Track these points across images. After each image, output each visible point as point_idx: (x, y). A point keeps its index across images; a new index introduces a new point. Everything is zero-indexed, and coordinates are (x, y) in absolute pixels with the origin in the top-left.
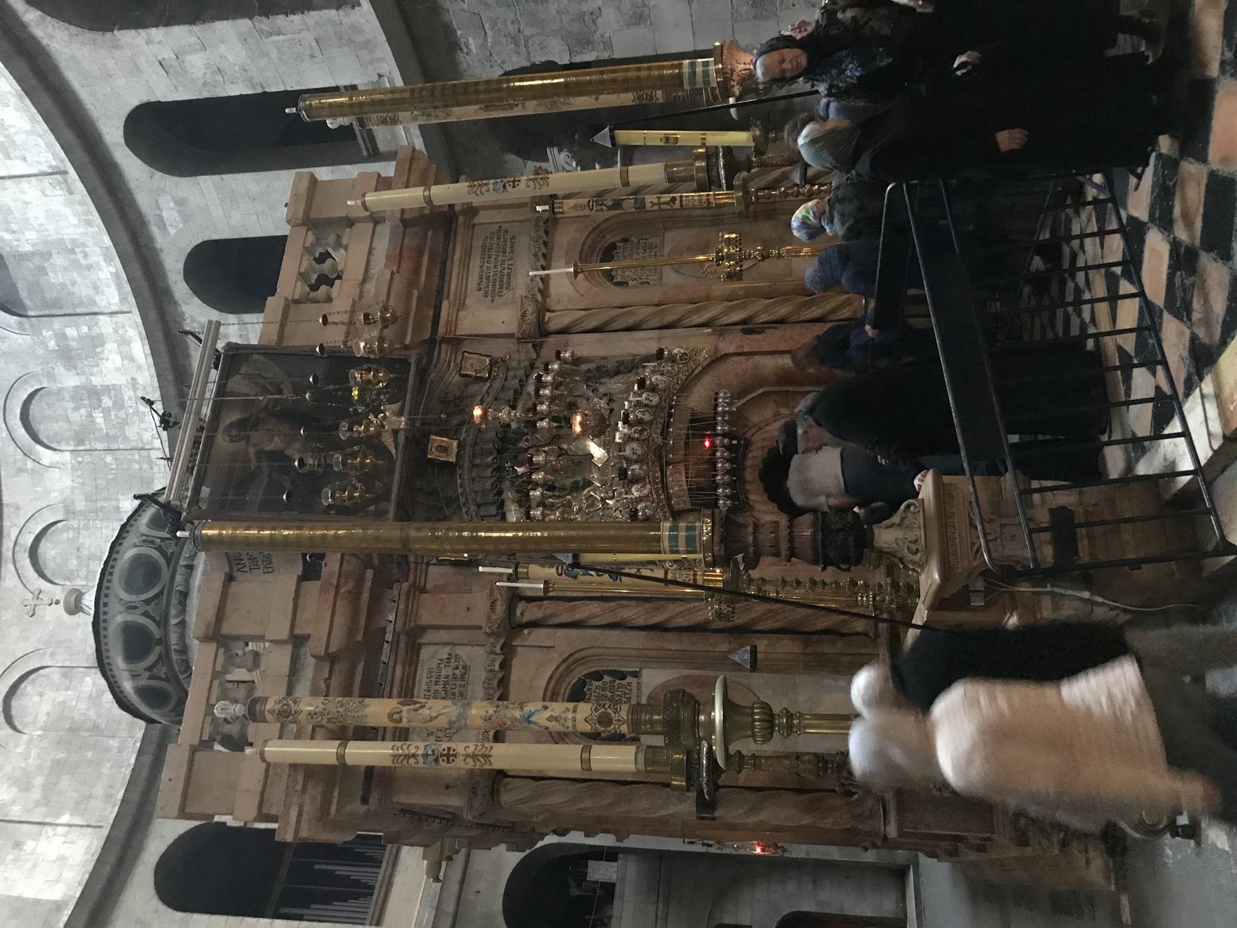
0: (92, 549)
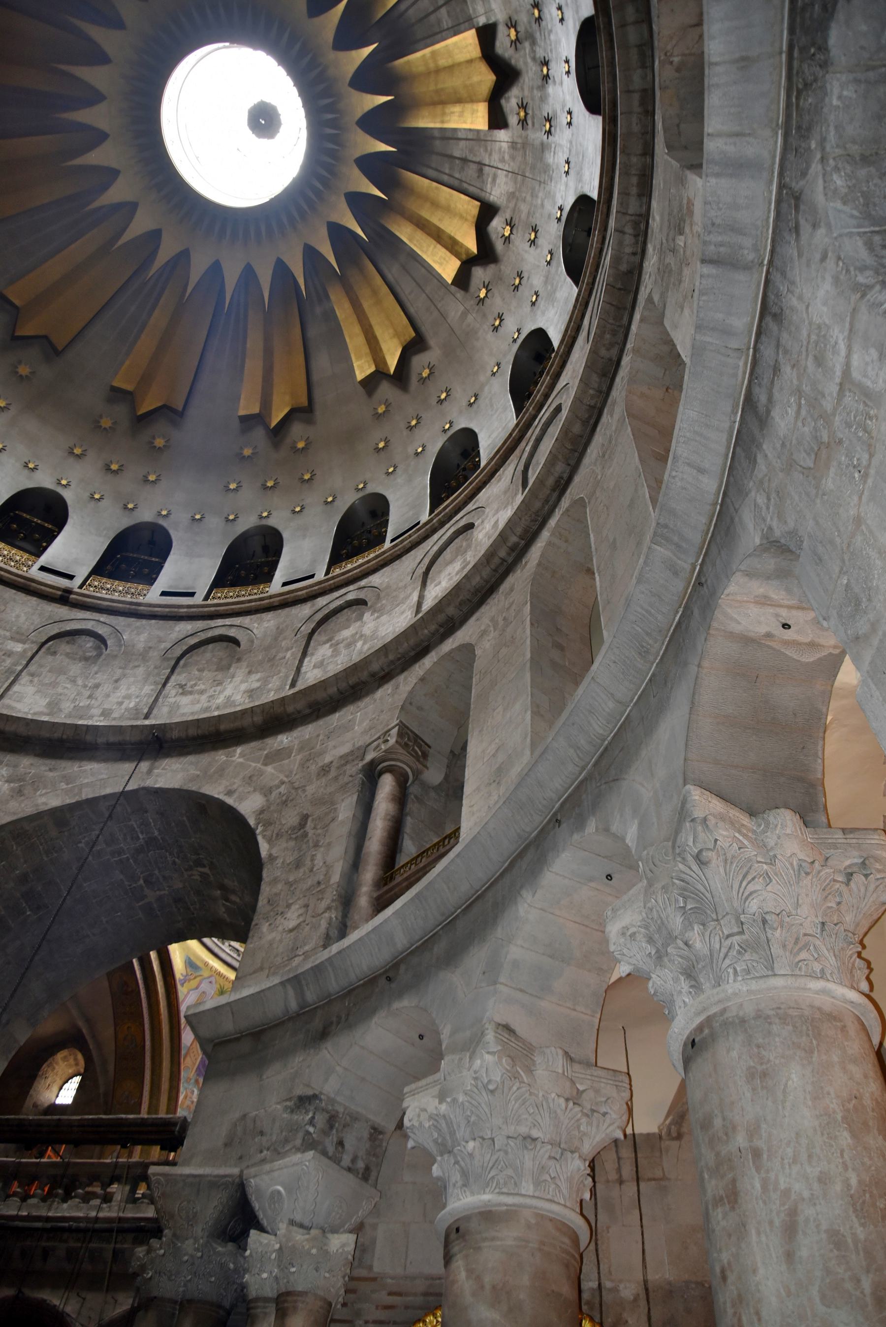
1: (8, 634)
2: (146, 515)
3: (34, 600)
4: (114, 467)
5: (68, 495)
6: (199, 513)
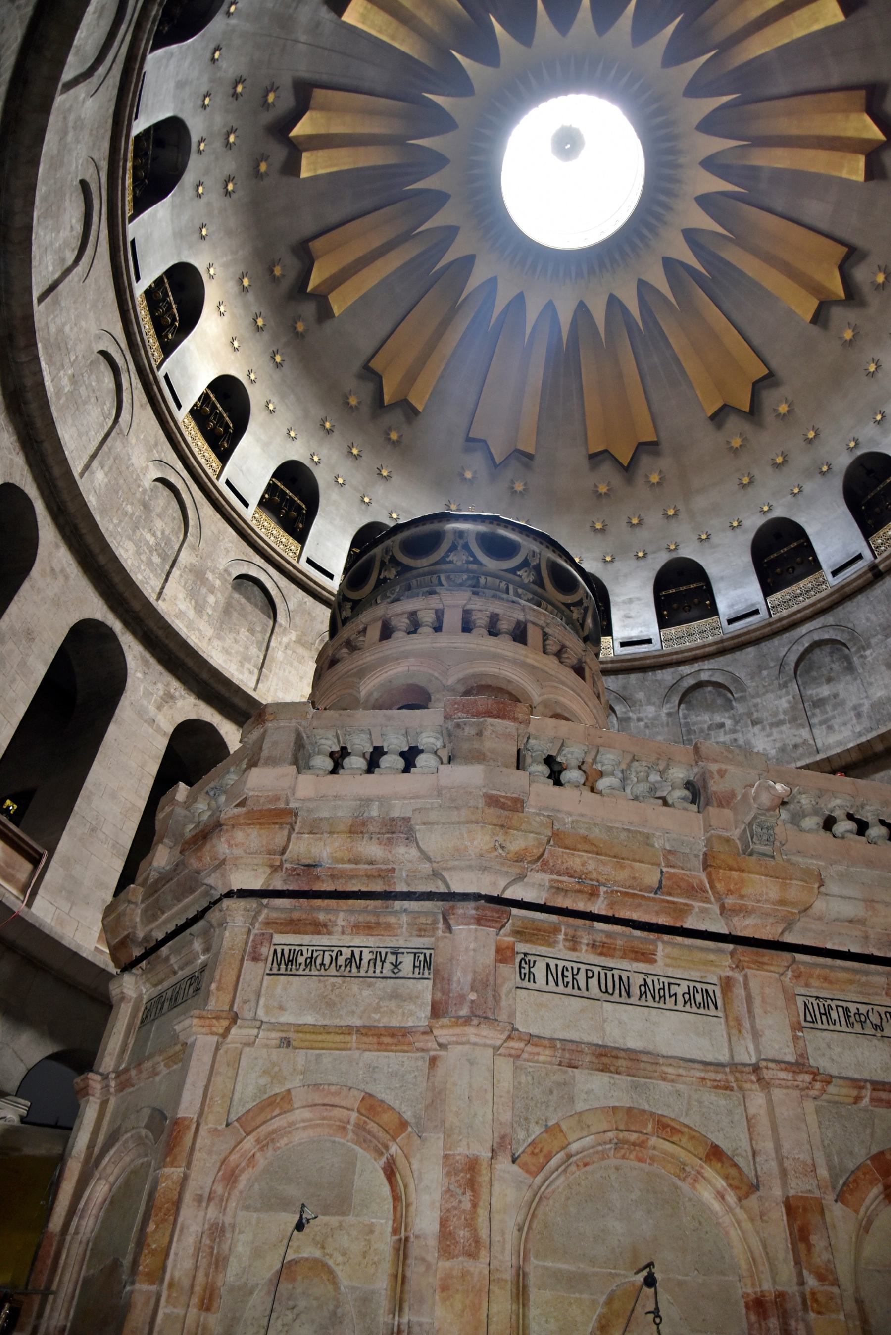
0: (90, 407)
1: (880, 637)
2: (844, 461)
3: (860, 598)
4: (779, 460)
5: (778, 513)
6: (876, 414)
